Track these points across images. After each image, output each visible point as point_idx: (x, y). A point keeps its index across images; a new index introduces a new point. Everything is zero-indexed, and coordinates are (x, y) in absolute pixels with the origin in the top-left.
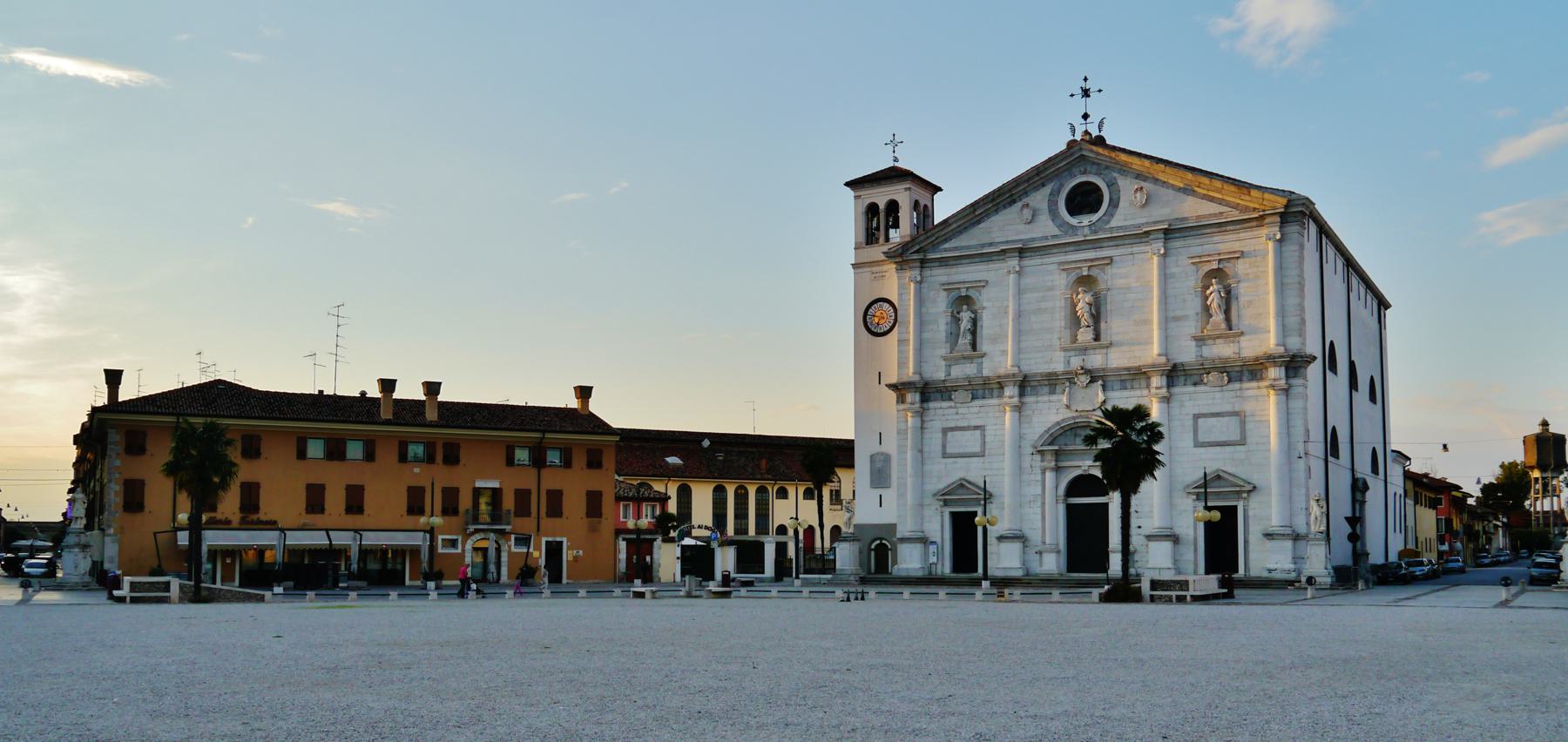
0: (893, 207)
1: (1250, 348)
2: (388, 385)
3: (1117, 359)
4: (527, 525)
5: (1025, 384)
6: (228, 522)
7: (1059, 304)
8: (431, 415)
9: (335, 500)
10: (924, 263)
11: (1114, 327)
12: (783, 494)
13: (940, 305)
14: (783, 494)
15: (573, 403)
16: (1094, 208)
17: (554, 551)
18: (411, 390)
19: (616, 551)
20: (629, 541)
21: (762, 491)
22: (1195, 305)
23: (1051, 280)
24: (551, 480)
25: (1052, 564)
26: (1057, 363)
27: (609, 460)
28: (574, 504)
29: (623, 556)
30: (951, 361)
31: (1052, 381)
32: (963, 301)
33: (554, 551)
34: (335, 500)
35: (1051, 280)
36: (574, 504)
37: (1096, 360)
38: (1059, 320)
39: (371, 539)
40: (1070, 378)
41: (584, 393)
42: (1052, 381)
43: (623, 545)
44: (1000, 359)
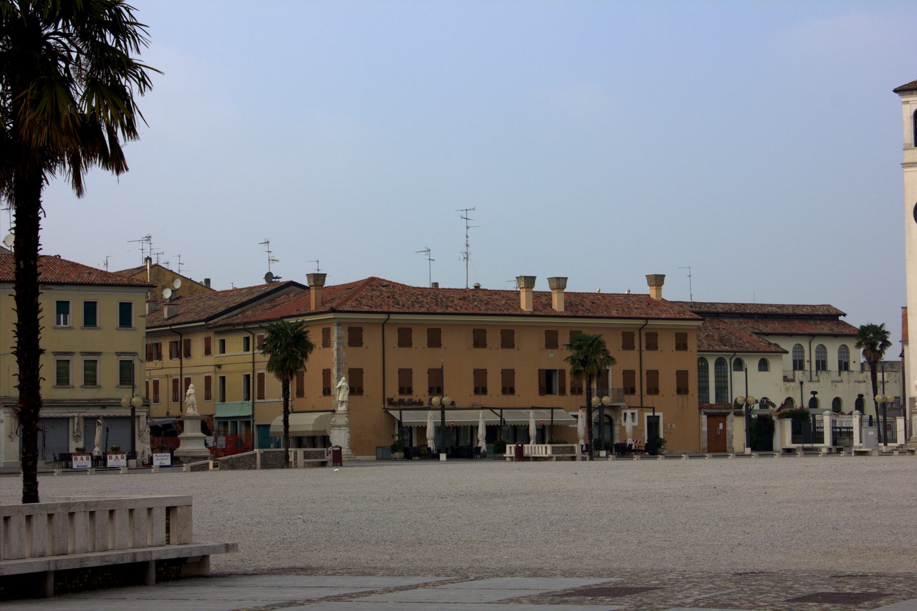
2: (529, 281)
4: (635, 399)
6: (421, 403)
8: (558, 304)
9: (494, 383)
12: (739, 365)
14: (739, 365)
15: (643, 288)
17: (653, 423)
18: (541, 285)
19: (700, 425)
20: (710, 416)
21: (720, 363)
24: (652, 360)
27: (692, 343)
28: (668, 383)
29: (705, 428)
33: (653, 423)
34: (494, 383)
36: (668, 383)
39: (453, 417)
41: (657, 281)
43: (704, 418)
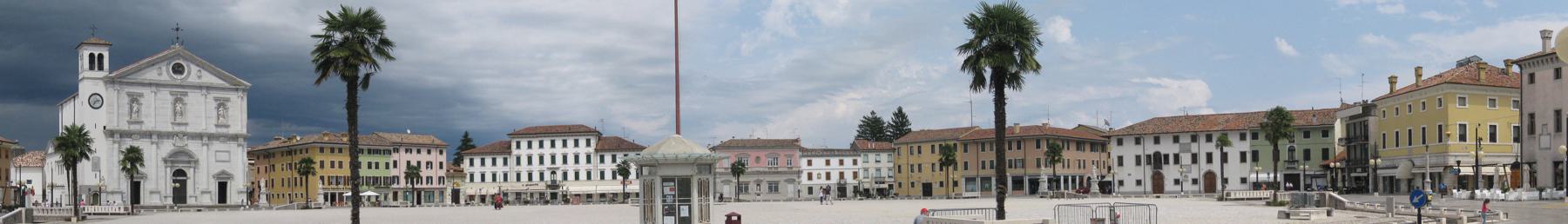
0: (101, 56)
1: (232, 131)
3: (189, 129)
5: (161, 135)
7: (169, 106)
10: (121, 83)
11: (189, 118)
13: (126, 100)
16: (181, 73)
22: (215, 113)
23: (166, 96)
25: (170, 201)
26: (170, 129)
30: (130, 123)
31: (169, 135)
32: (134, 99)
35: (166, 96)
37: (183, 129)
38: (170, 112)
40: (176, 134)
42: (169, 135)
44: (148, 125)
